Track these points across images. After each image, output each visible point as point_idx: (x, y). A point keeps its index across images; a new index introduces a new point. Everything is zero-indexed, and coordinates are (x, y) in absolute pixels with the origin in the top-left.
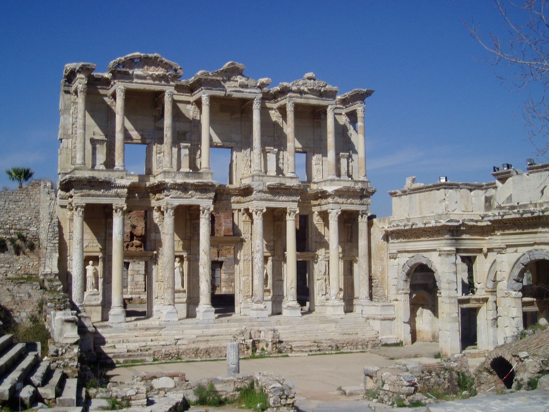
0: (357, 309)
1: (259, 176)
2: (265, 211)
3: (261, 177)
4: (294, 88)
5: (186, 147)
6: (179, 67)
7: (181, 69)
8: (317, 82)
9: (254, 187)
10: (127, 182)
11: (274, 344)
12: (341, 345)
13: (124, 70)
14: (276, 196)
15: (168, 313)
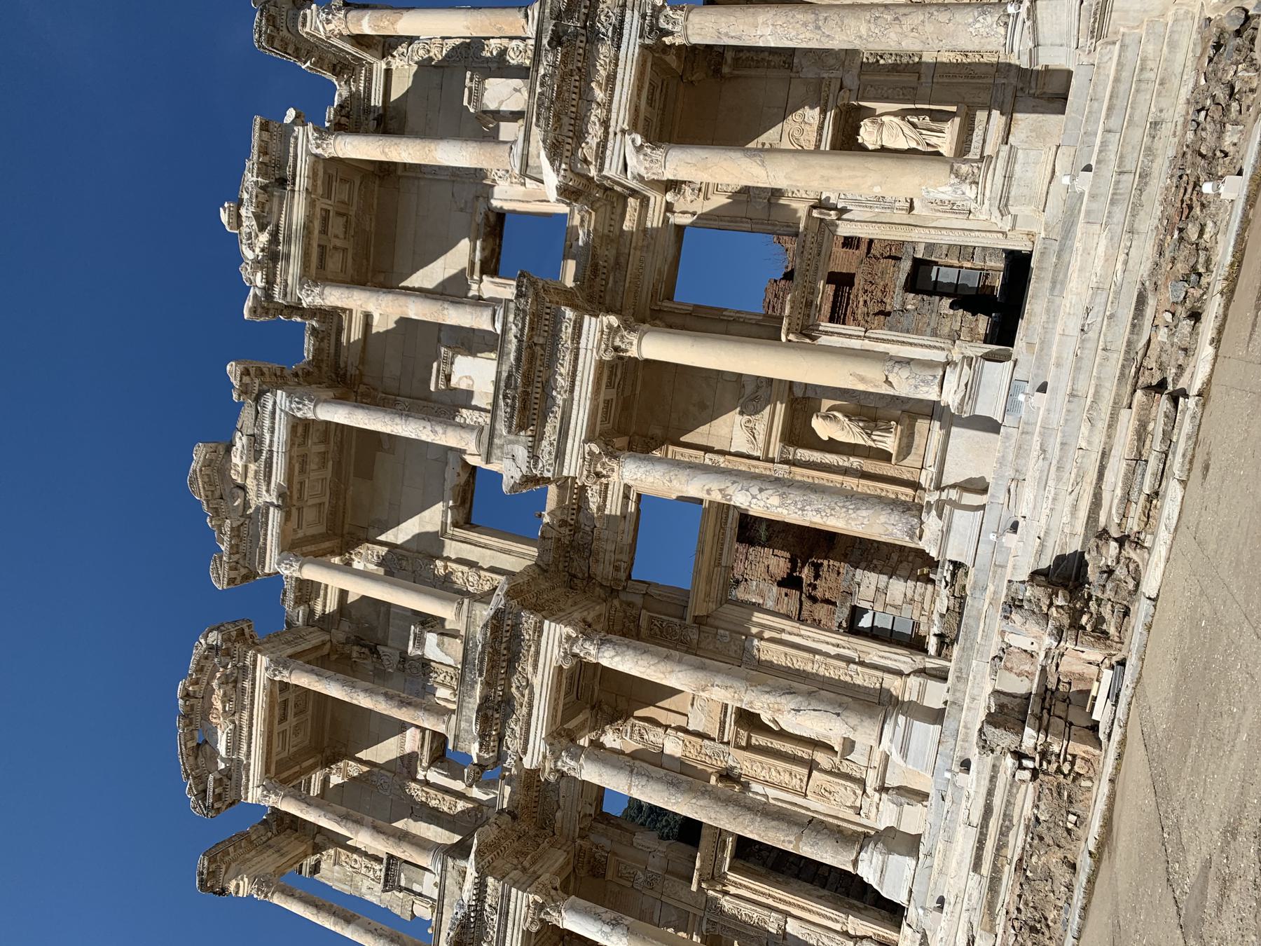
0: (1051, 58)
1: (491, 443)
2: (596, 449)
3: (496, 441)
4: (259, 280)
5: (420, 641)
6: (203, 641)
7: (206, 637)
8: (245, 196)
9: (518, 476)
10: (470, 866)
11: (1076, 626)
12: (1185, 251)
13: (211, 784)
14: (554, 398)
15: (881, 882)
